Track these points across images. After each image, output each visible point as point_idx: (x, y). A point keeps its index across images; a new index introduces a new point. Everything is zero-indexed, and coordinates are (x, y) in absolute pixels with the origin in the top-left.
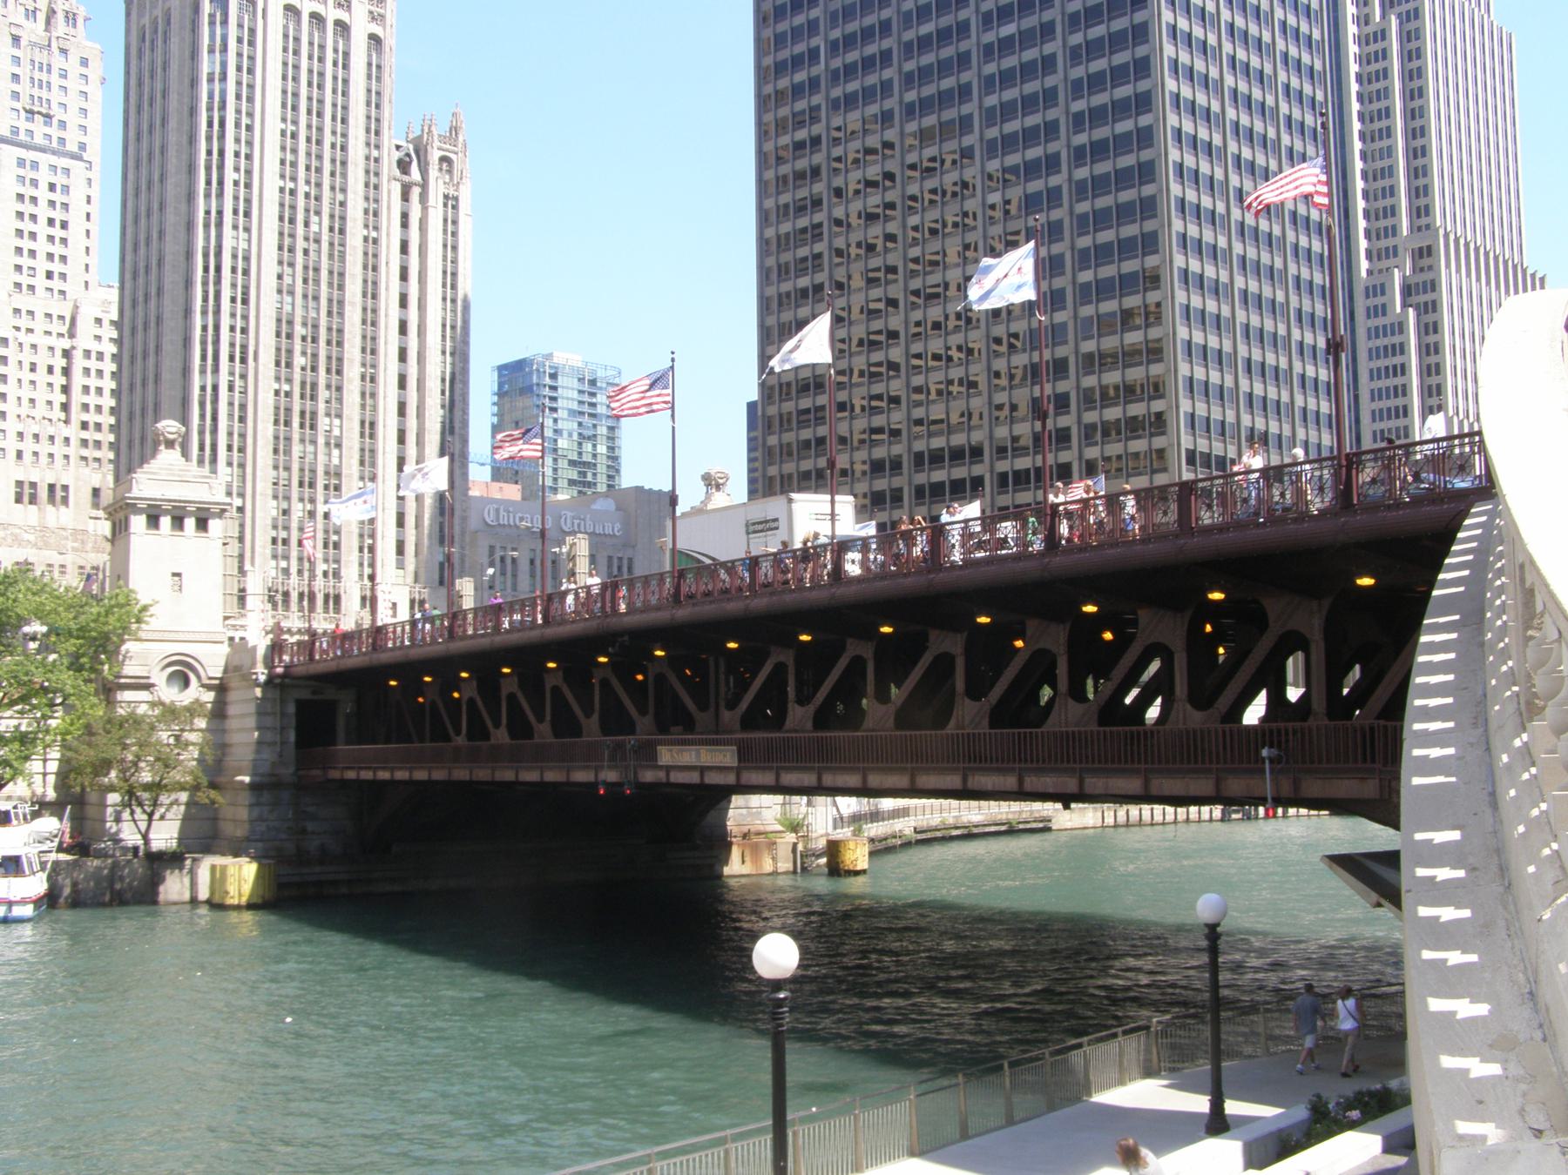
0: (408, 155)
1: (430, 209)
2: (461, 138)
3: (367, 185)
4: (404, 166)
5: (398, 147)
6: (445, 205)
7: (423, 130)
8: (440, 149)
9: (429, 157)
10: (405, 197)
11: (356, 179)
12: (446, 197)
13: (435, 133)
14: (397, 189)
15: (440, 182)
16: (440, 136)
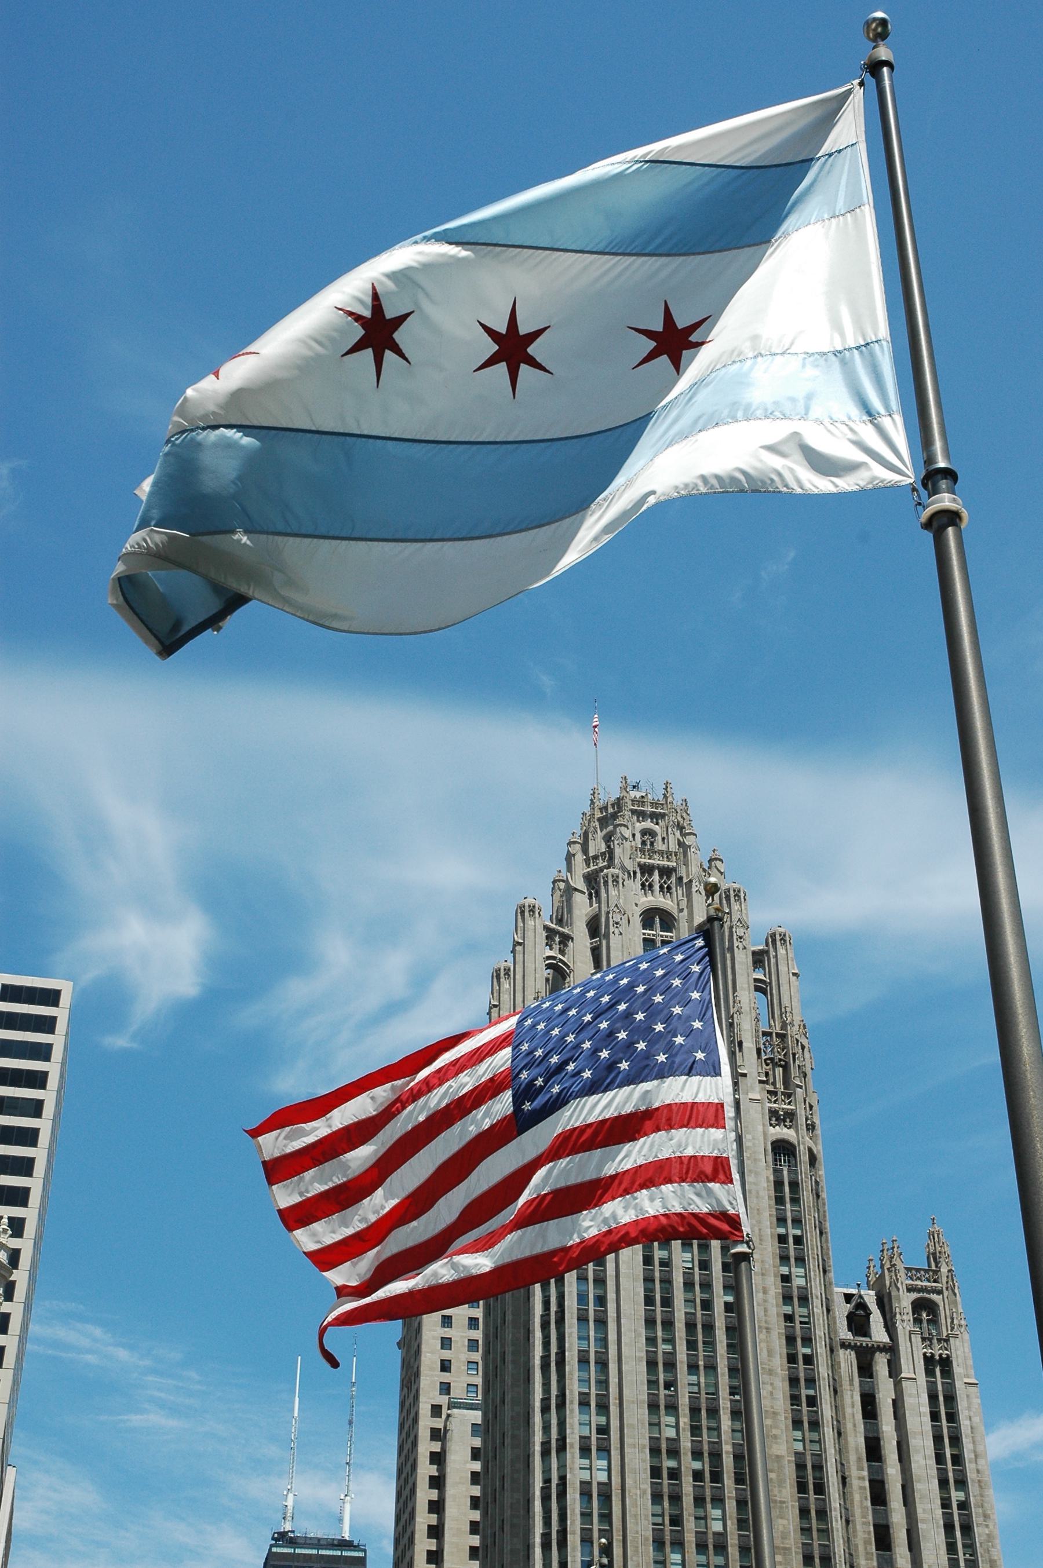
0: (862, 1306)
1: (904, 1383)
2: (944, 1270)
3: (792, 1358)
4: (858, 1322)
5: (848, 1298)
6: (929, 1372)
7: (882, 1266)
8: (911, 1289)
9: (895, 1304)
10: (866, 1369)
11: (770, 1353)
12: (929, 1360)
13: (900, 1266)
14: (847, 1359)
15: (917, 1339)
16: (908, 1269)
